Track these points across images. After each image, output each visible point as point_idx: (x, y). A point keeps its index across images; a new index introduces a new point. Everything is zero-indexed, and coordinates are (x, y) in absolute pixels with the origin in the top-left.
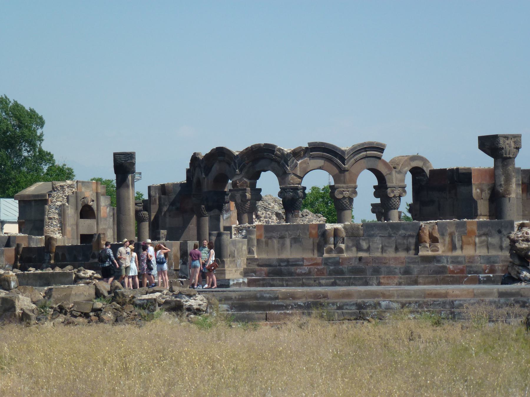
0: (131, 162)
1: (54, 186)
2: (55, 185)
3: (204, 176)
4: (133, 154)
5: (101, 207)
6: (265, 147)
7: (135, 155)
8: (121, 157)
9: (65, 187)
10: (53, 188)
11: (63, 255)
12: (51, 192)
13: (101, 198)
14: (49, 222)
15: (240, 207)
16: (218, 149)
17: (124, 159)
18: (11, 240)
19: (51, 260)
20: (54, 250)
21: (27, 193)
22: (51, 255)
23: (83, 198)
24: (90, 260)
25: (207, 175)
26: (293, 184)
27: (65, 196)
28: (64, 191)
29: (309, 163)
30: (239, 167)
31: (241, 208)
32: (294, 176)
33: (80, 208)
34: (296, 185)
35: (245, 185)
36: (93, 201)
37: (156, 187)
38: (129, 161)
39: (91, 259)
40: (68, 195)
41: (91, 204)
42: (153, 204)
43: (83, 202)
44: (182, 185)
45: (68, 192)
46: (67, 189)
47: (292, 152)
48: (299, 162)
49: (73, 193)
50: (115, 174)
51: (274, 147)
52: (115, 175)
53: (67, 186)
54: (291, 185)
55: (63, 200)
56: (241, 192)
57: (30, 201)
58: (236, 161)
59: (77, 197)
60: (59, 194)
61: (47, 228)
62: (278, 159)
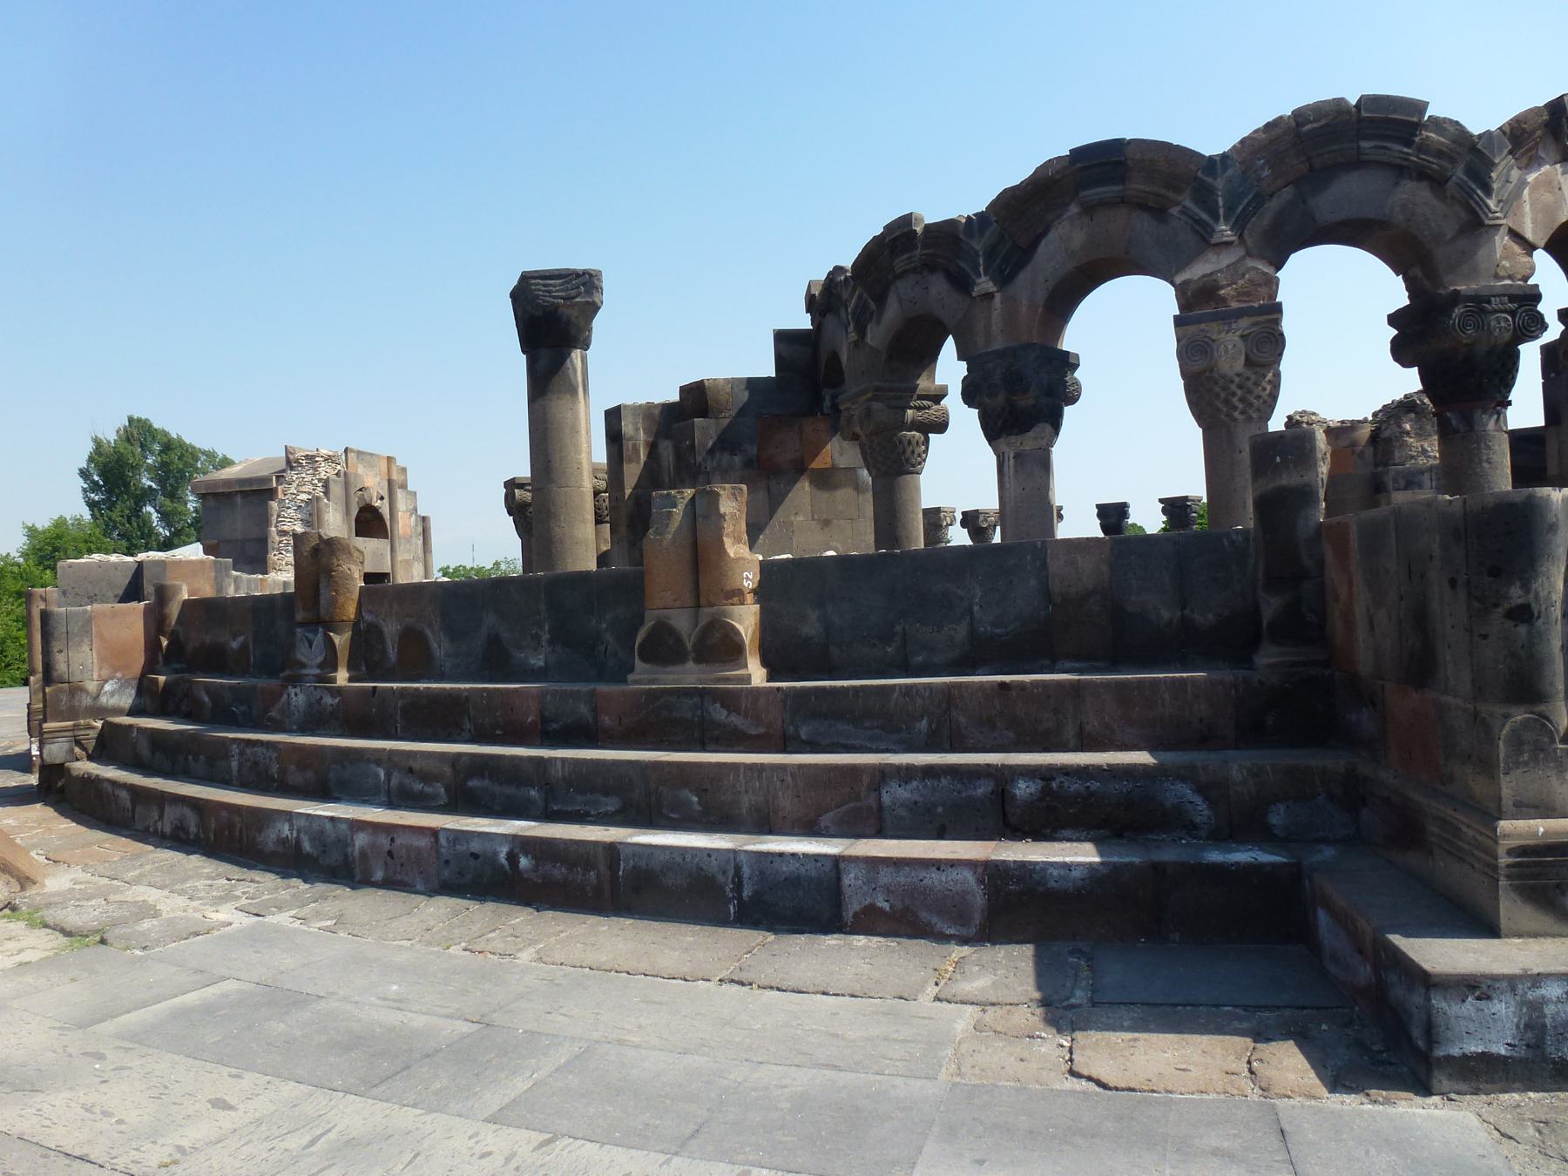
0: (588, 302)
1: (291, 457)
2: (292, 454)
3: (984, 284)
4: (593, 272)
5: (400, 513)
6: (1367, 110)
7: (600, 280)
8: (550, 285)
9: (317, 459)
10: (288, 462)
11: (412, 639)
12: (284, 471)
13: (399, 494)
14: (280, 542)
15: (1239, 392)
16: (1079, 154)
17: (562, 290)
18: (146, 573)
19: (336, 670)
20: (351, 611)
21: (223, 477)
22: (337, 639)
23: (360, 490)
24: (632, 669)
25: (1004, 279)
26: (1510, 277)
27: (320, 480)
28: (315, 470)
29: (1563, 187)
30: (1230, 209)
31: (1242, 400)
32: (1512, 243)
33: (354, 513)
34: (1519, 282)
35: (1263, 291)
36: (382, 498)
37: (636, 409)
38: (578, 300)
39: (638, 664)
40: (325, 477)
41: (376, 505)
42: (630, 461)
43: (362, 498)
44: (752, 384)
45: (325, 470)
46: (323, 465)
47: (1508, 130)
48: (1531, 178)
49: (338, 474)
50: (523, 352)
51: (1420, 107)
52: (522, 360)
53: (322, 457)
54: (1503, 278)
55: (313, 489)
56: (1244, 323)
57: (229, 496)
58: (1220, 184)
59: (347, 485)
60: (304, 475)
61: (275, 555)
62: (1435, 164)
